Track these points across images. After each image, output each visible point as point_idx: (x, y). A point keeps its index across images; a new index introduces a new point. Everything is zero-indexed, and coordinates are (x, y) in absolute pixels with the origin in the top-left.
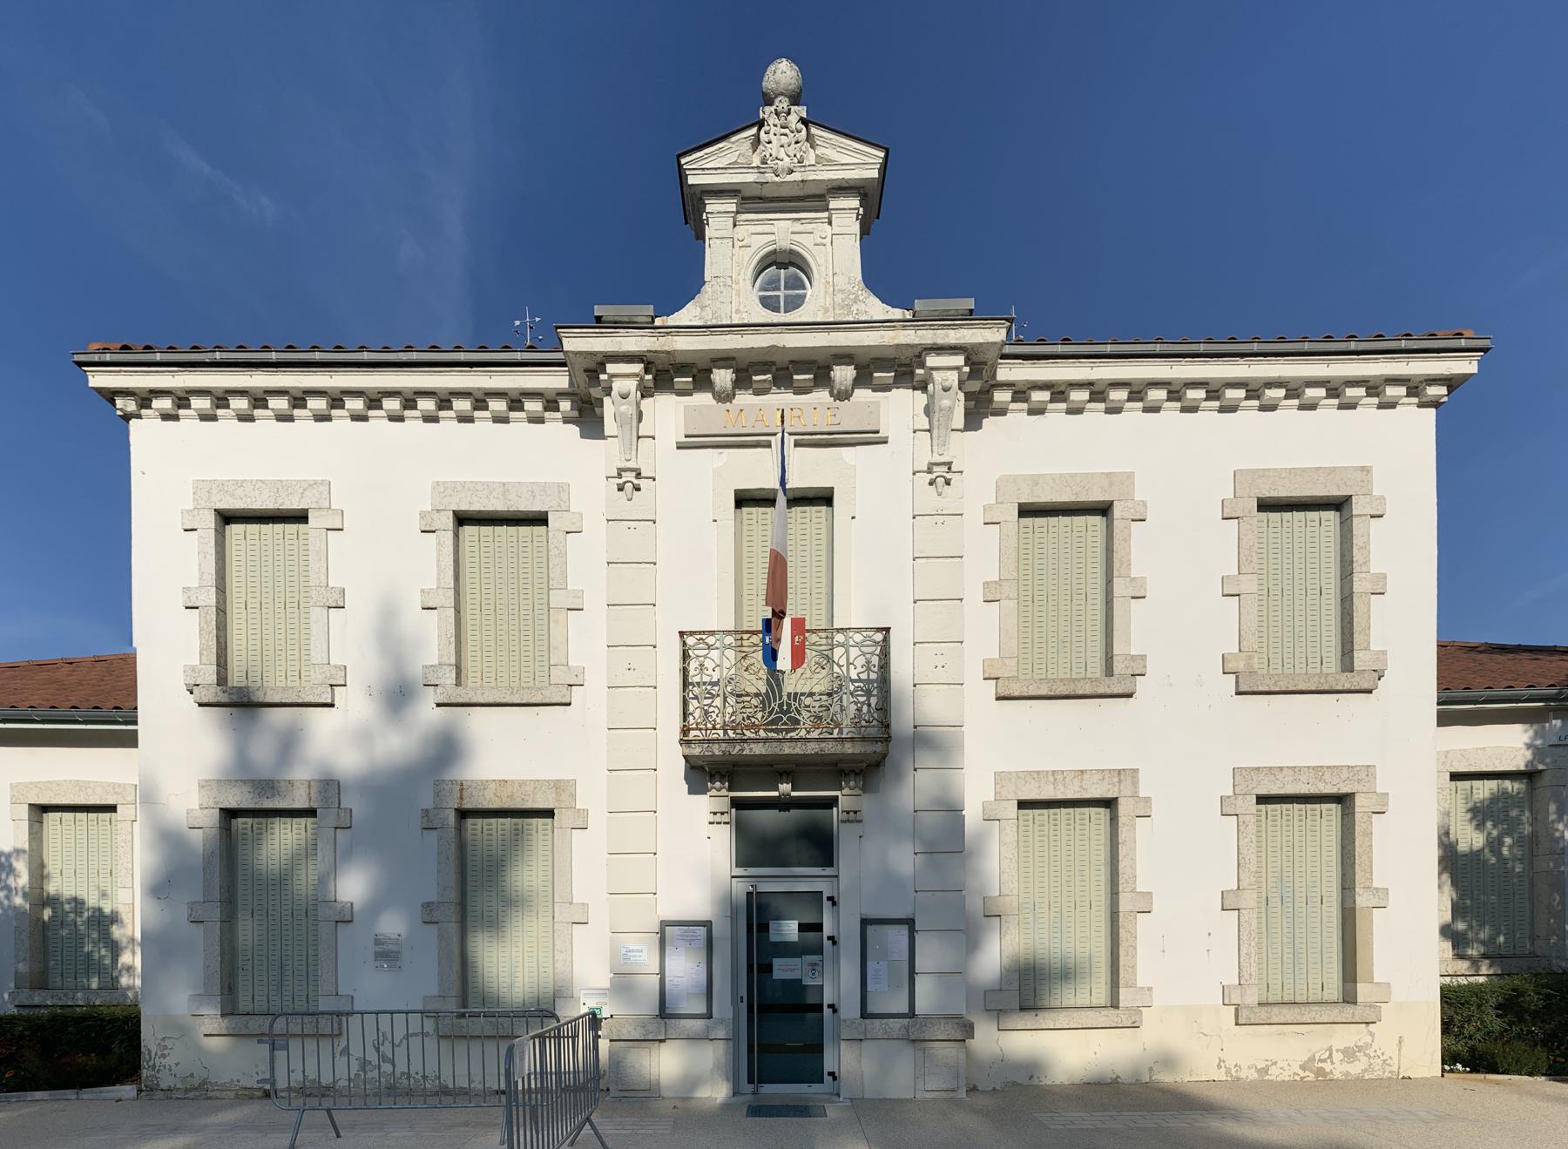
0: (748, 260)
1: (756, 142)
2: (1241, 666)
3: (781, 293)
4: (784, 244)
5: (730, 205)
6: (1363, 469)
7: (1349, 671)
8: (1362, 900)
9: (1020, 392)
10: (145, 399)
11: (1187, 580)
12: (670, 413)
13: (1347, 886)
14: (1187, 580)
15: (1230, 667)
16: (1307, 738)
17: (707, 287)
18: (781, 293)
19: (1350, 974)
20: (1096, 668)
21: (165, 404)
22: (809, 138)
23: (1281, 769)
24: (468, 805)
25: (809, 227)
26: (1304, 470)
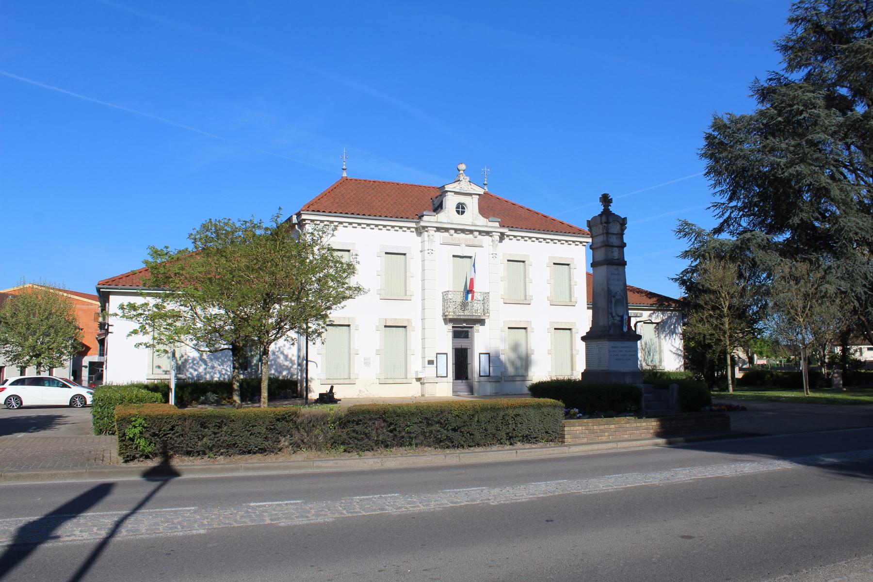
4: (462, 202)
7: (571, 304)
8: (574, 353)
9: (508, 236)
11: (540, 279)
12: (440, 236)
13: (572, 349)
14: (540, 279)
16: (564, 316)
19: (572, 370)
20: (523, 298)
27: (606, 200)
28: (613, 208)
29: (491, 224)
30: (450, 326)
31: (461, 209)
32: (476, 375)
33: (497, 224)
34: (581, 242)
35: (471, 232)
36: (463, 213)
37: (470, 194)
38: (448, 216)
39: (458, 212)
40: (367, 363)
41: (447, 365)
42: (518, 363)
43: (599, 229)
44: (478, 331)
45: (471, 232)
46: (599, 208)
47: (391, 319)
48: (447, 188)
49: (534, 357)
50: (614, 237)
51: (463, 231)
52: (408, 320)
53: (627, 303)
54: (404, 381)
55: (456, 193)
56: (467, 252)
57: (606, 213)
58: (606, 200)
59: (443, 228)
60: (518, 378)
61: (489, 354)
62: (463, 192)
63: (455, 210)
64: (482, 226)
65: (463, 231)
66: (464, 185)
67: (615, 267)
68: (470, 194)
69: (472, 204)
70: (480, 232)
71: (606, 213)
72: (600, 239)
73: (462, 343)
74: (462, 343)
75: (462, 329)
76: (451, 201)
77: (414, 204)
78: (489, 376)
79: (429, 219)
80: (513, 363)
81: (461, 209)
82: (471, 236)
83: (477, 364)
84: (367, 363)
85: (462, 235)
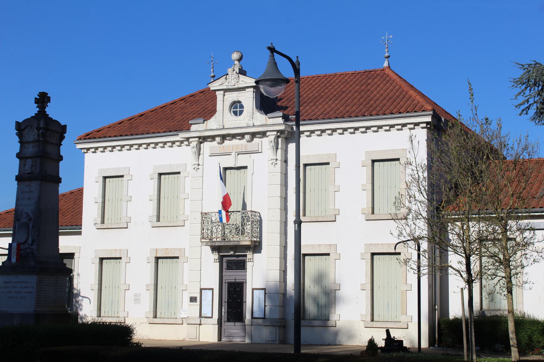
0: (228, 104)
1: (226, 79)
2: (366, 212)
3: (238, 110)
4: (236, 100)
5: (222, 92)
6: (403, 149)
10: (88, 149)
15: (364, 212)
17: (217, 113)
18: (238, 110)
21: (93, 150)
22: (239, 77)
23: (378, 244)
24: (158, 256)
25: (243, 94)
26: (385, 151)
27: (43, 100)
28: (51, 111)
29: (271, 121)
30: (216, 256)
31: (237, 108)
32: (248, 316)
33: (281, 121)
34: (417, 124)
35: (242, 136)
36: (241, 112)
37: (243, 89)
38: (222, 120)
39: (235, 113)
40: (137, 300)
41: (211, 304)
42: (323, 300)
43: (31, 135)
44: (252, 260)
45: (242, 135)
46: (33, 110)
47: (162, 249)
48: (214, 86)
49: (344, 292)
50: (31, 145)
51: (233, 136)
52: (180, 250)
53: (58, 226)
54: (173, 321)
55: (226, 90)
56: (242, 161)
57: (42, 115)
58: (43, 100)
59: (209, 137)
60: (317, 323)
61: (265, 289)
62: (235, 89)
63: (245, 109)
64: (248, 127)
65: (233, 136)
66: (233, 79)
67: (27, 183)
68: (243, 89)
69: (248, 99)
70: (253, 135)
71: (42, 115)
72: (31, 150)
73: (232, 276)
74: (232, 276)
75: (233, 257)
76: (223, 102)
77: (176, 116)
78: (264, 318)
79: (198, 128)
80: (316, 300)
81: (237, 108)
82: (244, 141)
83: (253, 301)
84: (137, 300)
85: (235, 142)
